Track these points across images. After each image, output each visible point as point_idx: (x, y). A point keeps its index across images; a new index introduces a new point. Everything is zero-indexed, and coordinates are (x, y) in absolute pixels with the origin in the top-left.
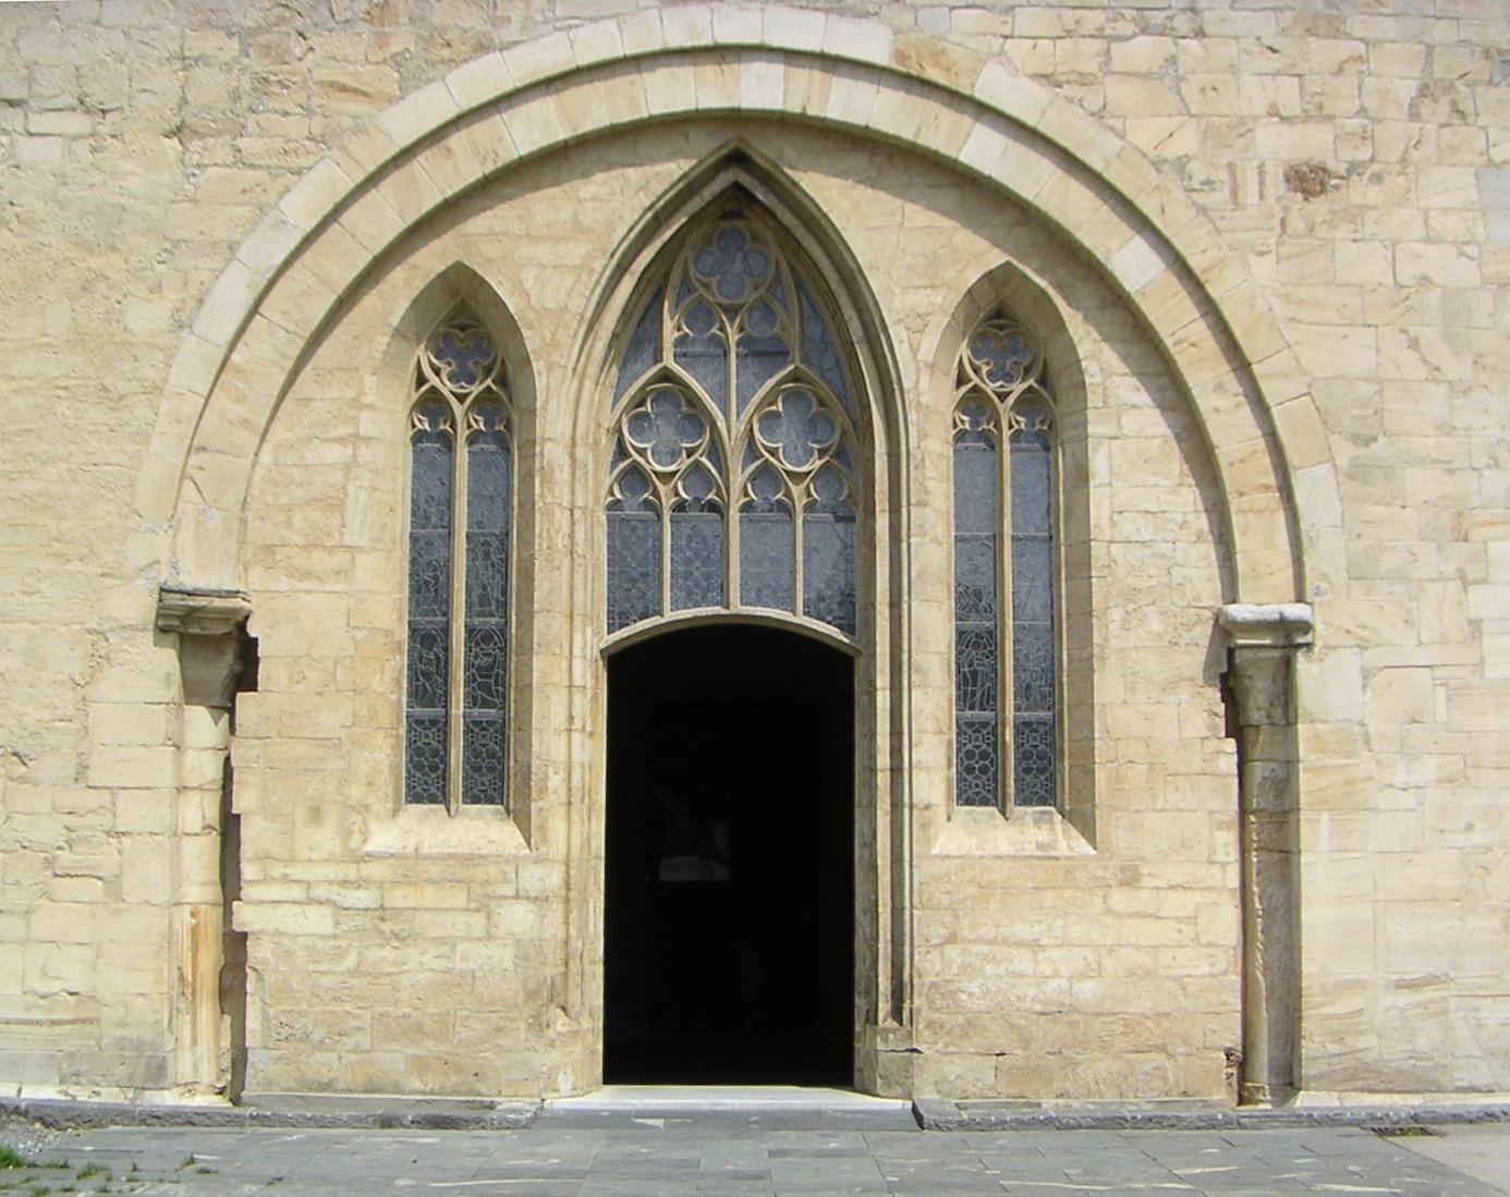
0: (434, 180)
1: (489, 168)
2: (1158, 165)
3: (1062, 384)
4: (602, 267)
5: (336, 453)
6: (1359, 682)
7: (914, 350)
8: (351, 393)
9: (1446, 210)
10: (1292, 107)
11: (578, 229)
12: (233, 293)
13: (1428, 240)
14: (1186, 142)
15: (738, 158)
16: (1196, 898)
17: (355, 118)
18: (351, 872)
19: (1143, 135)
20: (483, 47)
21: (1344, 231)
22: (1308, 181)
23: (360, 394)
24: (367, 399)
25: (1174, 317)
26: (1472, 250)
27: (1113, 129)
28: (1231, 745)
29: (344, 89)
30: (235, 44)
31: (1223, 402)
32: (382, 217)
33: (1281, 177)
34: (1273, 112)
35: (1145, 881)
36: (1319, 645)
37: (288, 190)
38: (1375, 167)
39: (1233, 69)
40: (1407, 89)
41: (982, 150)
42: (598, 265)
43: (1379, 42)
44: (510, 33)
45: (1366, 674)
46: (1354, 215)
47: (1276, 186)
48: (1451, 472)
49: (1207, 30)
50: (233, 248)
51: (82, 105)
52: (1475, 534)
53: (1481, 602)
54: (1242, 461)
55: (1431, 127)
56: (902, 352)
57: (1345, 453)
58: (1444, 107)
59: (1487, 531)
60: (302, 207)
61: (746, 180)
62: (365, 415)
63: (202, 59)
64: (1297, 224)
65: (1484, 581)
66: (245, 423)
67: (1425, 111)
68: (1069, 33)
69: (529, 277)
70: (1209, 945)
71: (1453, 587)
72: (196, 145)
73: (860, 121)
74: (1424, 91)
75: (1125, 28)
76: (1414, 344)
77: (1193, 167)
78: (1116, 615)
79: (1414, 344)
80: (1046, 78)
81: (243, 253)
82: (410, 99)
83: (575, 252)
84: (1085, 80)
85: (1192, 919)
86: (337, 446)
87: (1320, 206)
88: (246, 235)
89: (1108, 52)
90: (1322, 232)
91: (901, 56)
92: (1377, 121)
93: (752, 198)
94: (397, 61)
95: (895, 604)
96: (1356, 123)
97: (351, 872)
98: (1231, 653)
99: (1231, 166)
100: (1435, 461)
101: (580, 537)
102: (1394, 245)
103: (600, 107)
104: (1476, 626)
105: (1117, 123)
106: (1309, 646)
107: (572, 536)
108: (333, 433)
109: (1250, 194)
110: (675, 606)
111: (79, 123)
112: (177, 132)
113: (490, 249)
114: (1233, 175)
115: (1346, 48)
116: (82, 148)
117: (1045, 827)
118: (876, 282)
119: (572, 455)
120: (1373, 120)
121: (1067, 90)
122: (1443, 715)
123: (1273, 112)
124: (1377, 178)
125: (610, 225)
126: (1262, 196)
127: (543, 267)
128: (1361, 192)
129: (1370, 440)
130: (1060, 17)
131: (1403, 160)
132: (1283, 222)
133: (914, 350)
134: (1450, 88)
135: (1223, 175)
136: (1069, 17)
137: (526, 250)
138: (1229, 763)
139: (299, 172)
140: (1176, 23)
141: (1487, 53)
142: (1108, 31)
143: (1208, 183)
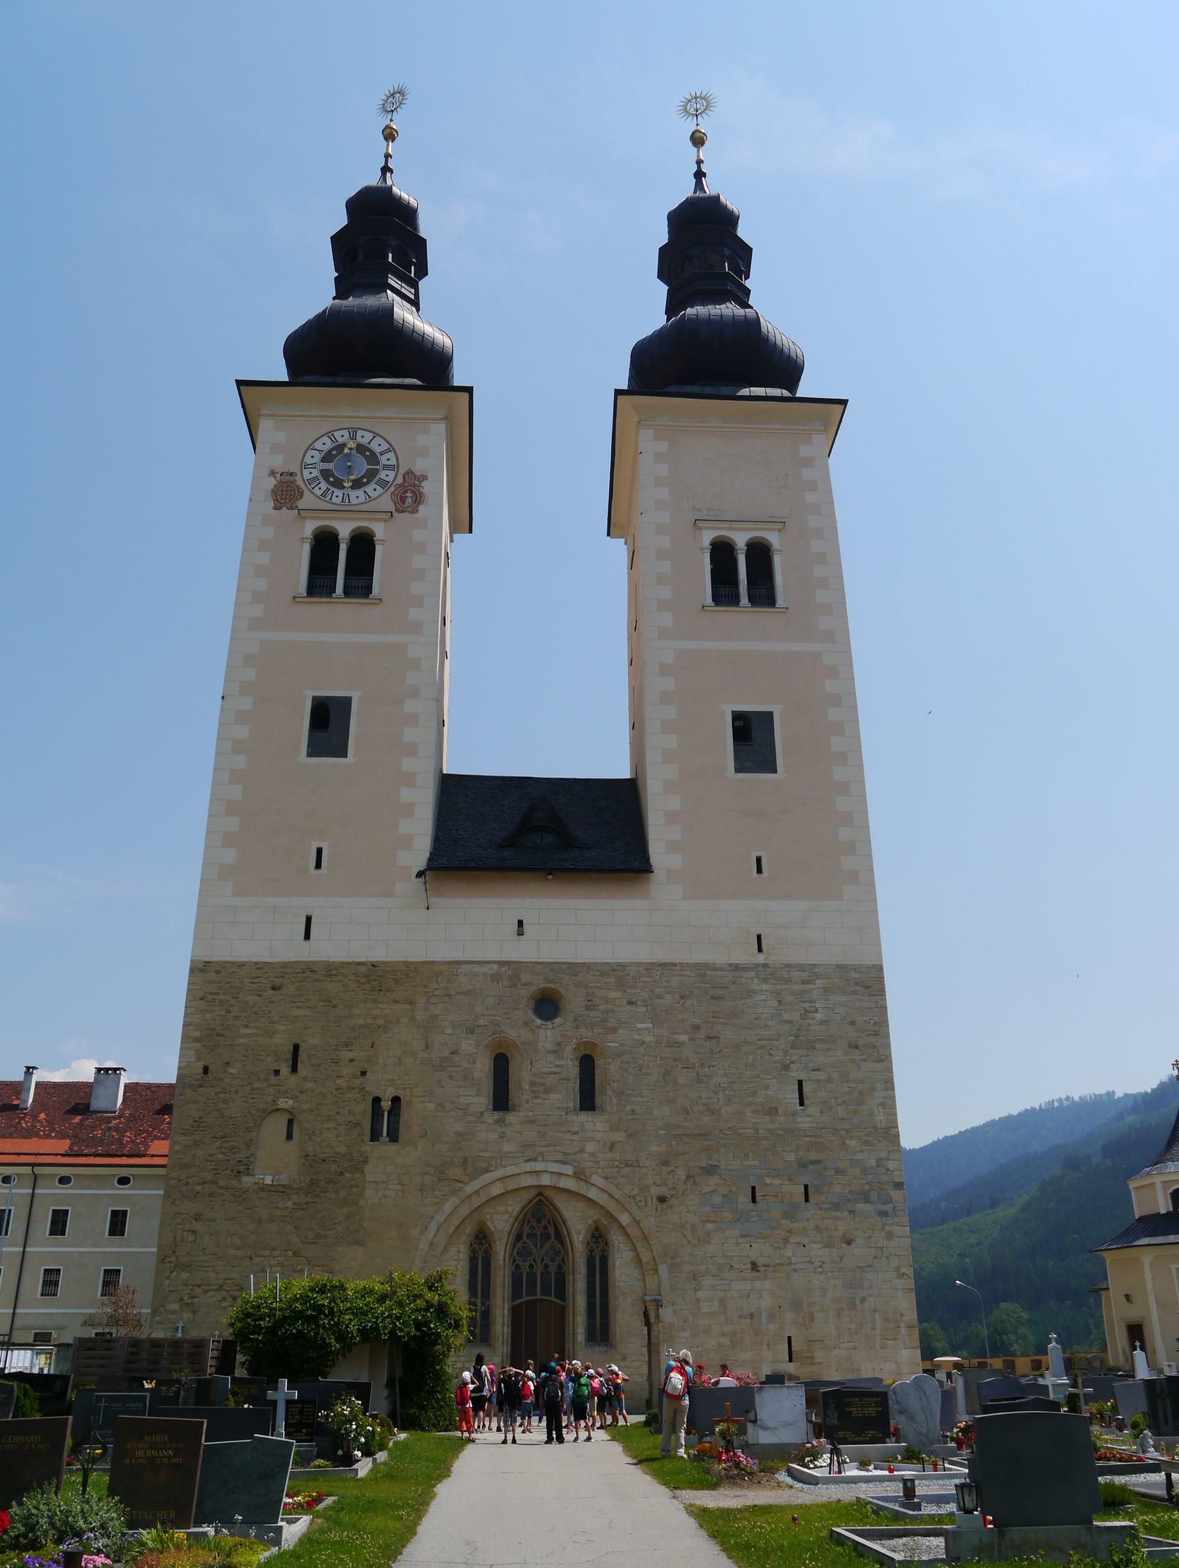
0: (476, 1202)
1: (488, 1199)
2: (629, 1197)
3: (610, 1244)
4: (512, 1220)
5: (454, 1263)
6: (672, 1313)
7: (578, 1239)
8: (458, 1249)
9: (692, 1205)
10: (658, 1182)
11: (506, 1212)
12: (433, 1227)
13: (688, 1212)
14: (635, 1192)
15: (540, 1194)
16: (638, 1363)
17: (460, 1187)
18: (457, 1359)
19: (626, 1191)
20: (487, 1171)
21: (669, 1211)
22: (662, 1199)
23: (460, 1249)
24: (461, 1250)
25: (634, 1232)
26: (698, 1214)
27: (619, 1189)
28: (646, 1328)
29: (457, 1180)
30: (433, 1170)
31: (644, 1250)
32: (465, 1211)
33: (656, 1198)
34: (655, 1184)
35: (628, 1360)
36: (664, 1305)
37: (445, 1203)
38: (676, 1196)
39: (647, 1175)
40: (683, 1178)
41: (592, 1194)
42: (511, 1220)
43: (676, 1167)
44: (492, 1169)
45: (674, 1312)
46: (671, 1207)
47: (655, 1198)
48: (692, 1265)
49: (641, 1165)
50: (433, 1217)
51: (400, 1183)
52: (699, 1279)
53: (700, 1294)
54: (648, 1263)
55: (689, 1186)
56: (575, 1239)
57: (669, 1261)
58: (692, 1180)
59: (701, 1278)
60: (448, 1207)
61: (542, 1198)
62: (460, 1254)
63: (427, 1173)
64: (659, 1209)
65: (700, 1290)
66: (435, 1256)
67: (688, 1182)
68: (611, 1167)
69: (496, 1222)
70: (642, 1374)
71: (693, 1291)
72: (425, 1193)
73: (566, 1188)
74: (688, 1177)
75: (623, 1166)
76: (685, 1236)
77: (637, 1197)
78: (621, 1298)
79: (685, 1236)
80: (606, 1178)
81: (435, 1218)
82: (471, 1183)
83: (505, 1217)
84: (615, 1178)
85: (638, 1368)
86: (455, 1261)
87: (664, 1206)
88: (436, 1213)
89: (619, 1171)
90: (664, 1211)
91: (575, 1173)
92: (677, 1185)
93: (543, 1202)
94: (468, 1175)
95: (573, 1296)
96: (672, 1186)
97: (457, 1359)
98: (646, 1306)
99: (645, 1196)
100: (689, 1263)
101: (506, 1281)
102: (680, 1213)
103: (512, 1185)
104: (698, 1300)
105: (621, 1187)
106: (662, 1306)
107: (504, 1281)
108: (454, 1258)
109: (649, 1204)
110: (527, 1295)
111: (399, 1187)
112: (421, 1190)
113: (488, 1217)
114: (645, 1199)
115: (670, 1168)
116: (400, 1194)
117: (606, 1347)
118: (570, 1223)
119: (504, 1262)
120: (677, 1185)
121: (610, 1180)
122: (691, 1321)
123: (655, 1184)
124: (677, 1198)
125: (513, 1211)
126: (652, 1203)
127: (498, 1220)
128: (674, 1201)
129: (673, 1258)
130: (609, 1163)
131: (683, 1194)
132: (656, 1209)
133: (578, 1239)
134: (693, 1176)
135: (644, 1199)
136: (611, 1163)
137: (495, 1217)
138: (645, 1332)
139: (447, 1200)
140: (634, 1164)
141: (701, 1168)
142: (620, 1166)
143: (640, 1201)
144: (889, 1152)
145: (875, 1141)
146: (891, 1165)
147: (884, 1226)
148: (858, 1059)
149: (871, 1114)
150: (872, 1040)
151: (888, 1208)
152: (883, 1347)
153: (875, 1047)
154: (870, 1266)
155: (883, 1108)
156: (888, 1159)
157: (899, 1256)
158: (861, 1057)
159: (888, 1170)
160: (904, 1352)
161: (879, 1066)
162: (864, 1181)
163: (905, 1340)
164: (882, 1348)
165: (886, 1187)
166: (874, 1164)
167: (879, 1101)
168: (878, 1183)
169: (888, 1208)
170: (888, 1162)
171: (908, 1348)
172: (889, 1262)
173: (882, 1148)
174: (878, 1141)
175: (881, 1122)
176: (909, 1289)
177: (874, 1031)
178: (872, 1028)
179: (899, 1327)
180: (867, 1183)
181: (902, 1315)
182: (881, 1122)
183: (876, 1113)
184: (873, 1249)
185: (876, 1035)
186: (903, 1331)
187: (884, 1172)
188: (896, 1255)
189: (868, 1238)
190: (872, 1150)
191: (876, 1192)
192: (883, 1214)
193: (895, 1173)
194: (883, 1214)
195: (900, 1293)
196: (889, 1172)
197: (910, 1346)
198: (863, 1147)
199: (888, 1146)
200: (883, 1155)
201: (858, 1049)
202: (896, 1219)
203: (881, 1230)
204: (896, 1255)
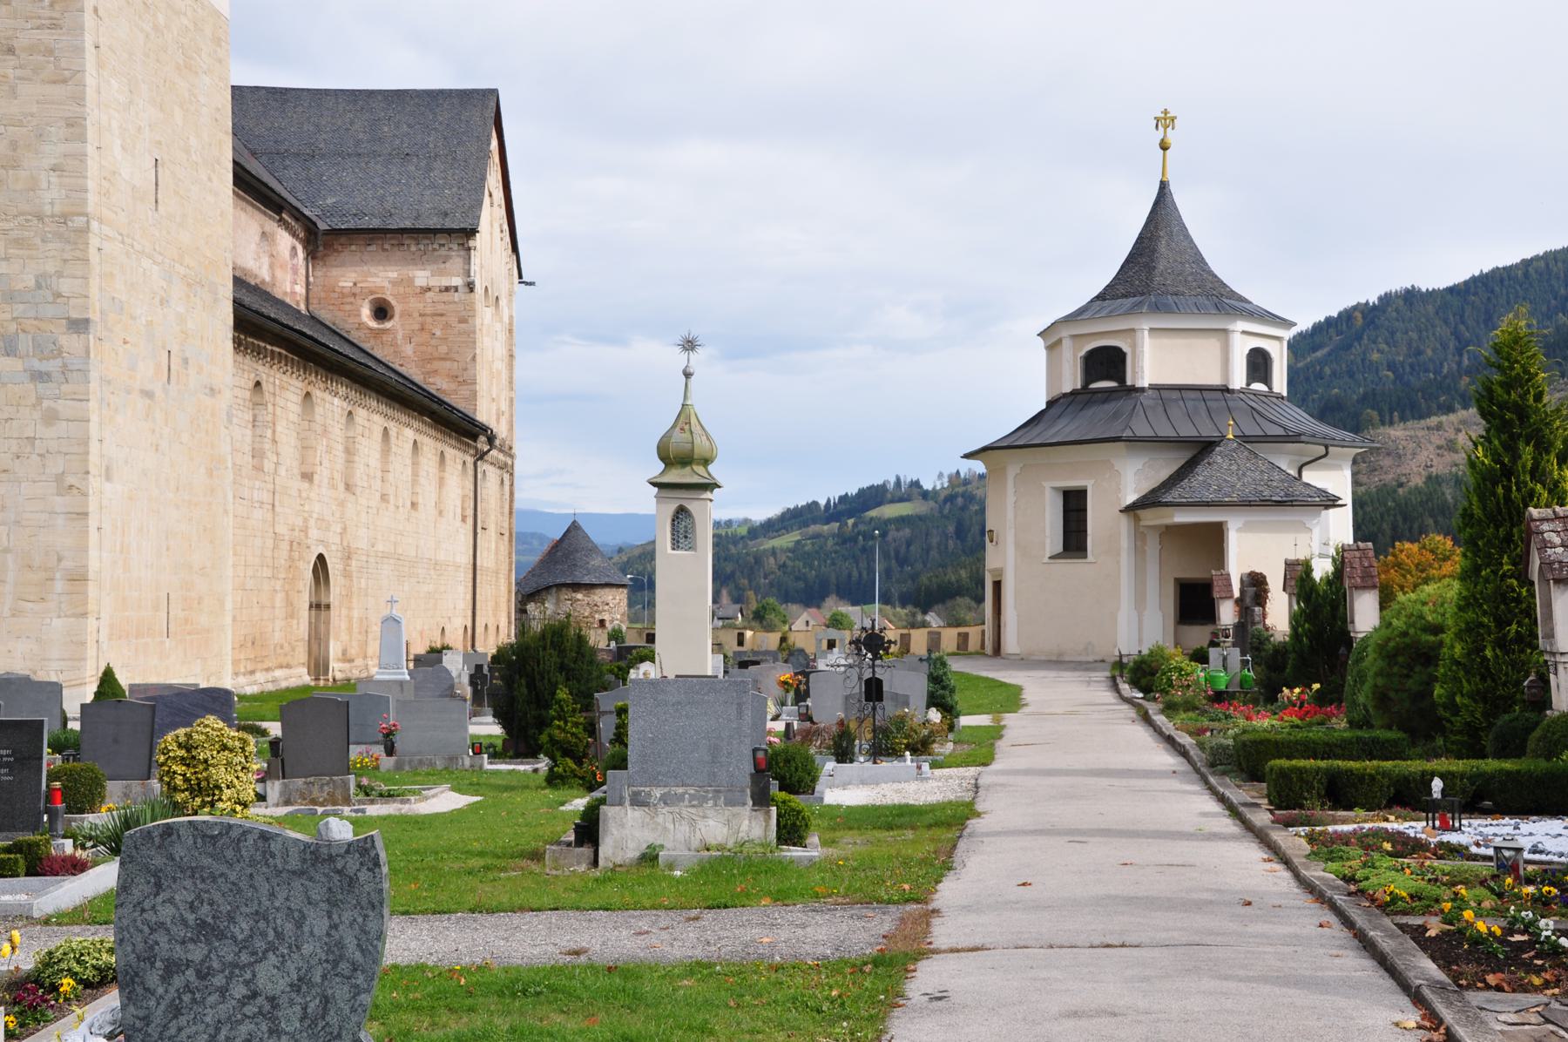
144: (65, 261)
145: (38, 241)
146: (65, 286)
147: (40, 399)
148: (12, 76)
149: (33, 187)
150: (46, 36)
151: (52, 366)
152: (16, 613)
153: (50, 52)
154: (5, 471)
155: (59, 176)
156: (60, 275)
157: (66, 454)
158: (18, 72)
159: (59, 295)
160: (57, 622)
161: (58, 91)
162: (8, 316)
163: (61, 603)
164: (13, 615)
165: (52, 327)
166: (32, 283)
167: (55, 161)
168: (36, 319)
169: (52, 366)
170: (61, 280)
171: (66, 616)
172: (43, 465)
173: (51, 253)
174: (43, 241)
175: (52, 204)
176: (78, 514)
177: (51, 18)
178: (47, 13)
179: (52, 580)
180: (14, 319)
181: (60, 560)
182: (52, 204)
183: (44, 185)
184: (15, 441)
185: (54, 26)
186: (59, 586)
187: (51, 299)
188: (60, 452)
189: (6, 420)
190: (31, 258)
191: (30, 337)
192: (40, 377)
193: (70, 303)
194: (40, 377)
195: (60, 521)
196: (59, 300)
197: (68, 613)
198: (11, 251)
199: (63, 250)
200: (50, 267)
201: (14, 54)
202: (64, 387)
203: (34, 406)
204: (60, 452)
